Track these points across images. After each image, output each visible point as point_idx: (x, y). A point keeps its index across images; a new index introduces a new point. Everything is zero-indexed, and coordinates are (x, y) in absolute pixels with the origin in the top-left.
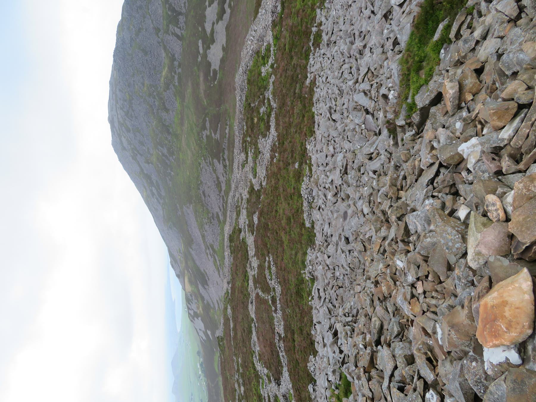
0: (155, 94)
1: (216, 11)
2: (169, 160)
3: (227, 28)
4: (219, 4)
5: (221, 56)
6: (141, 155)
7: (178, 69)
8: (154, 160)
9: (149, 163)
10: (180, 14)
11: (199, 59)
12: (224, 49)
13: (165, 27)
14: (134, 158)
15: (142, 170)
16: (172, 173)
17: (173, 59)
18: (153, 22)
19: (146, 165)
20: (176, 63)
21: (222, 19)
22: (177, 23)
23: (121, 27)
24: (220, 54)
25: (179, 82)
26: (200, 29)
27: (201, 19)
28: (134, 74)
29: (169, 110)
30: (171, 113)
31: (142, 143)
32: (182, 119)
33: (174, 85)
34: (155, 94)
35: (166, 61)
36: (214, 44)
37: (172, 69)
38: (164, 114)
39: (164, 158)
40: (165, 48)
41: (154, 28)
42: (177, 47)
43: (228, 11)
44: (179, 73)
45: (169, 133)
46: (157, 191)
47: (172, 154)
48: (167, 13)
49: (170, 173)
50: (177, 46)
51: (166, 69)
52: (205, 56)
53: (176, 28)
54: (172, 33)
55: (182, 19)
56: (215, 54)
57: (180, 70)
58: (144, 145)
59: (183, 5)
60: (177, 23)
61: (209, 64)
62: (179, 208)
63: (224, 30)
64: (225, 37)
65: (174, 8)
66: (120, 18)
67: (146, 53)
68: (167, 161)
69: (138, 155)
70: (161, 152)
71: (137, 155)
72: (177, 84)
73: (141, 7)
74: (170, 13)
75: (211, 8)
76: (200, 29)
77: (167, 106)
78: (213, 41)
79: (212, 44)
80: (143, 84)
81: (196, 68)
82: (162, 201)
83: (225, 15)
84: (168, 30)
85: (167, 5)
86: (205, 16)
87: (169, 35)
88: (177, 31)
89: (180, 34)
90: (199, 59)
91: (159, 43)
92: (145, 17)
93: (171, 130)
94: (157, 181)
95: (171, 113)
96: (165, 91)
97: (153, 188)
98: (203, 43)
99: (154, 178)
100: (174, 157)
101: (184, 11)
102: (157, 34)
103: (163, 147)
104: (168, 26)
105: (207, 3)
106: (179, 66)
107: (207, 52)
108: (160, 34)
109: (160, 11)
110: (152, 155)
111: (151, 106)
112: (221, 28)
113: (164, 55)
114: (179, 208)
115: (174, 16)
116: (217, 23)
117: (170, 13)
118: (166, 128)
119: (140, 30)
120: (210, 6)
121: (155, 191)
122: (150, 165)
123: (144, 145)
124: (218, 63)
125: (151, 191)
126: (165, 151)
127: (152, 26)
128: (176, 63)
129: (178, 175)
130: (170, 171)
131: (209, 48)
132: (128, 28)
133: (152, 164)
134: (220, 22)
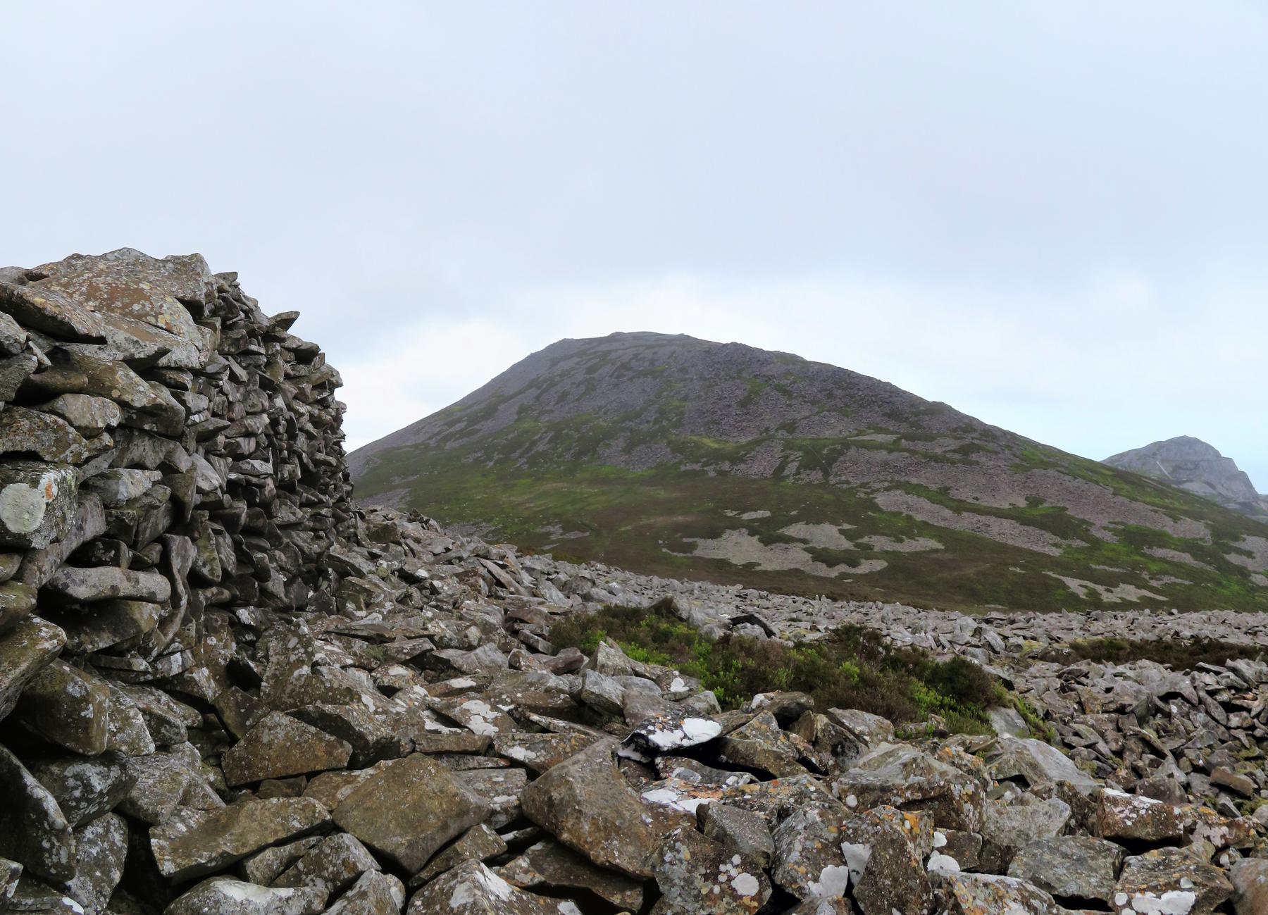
0: (665, 423)
1: (832, 546)
2: (521, 456)
3: (796, 573)
4: (847, 551)
5: (734, 561)
6: (538, 398)
7: (715, 470)
8: (527, 424)
9: (519, 413)
10: (826, 473)
11: (730, 513)
12: (749, 567)
13: (798, 442)
14: (533, 384)
15: (505, 400)
16: (491, 464)
17: (735, 458)
19: (516, 408)
20: (726, 466)
21: (814, 559)
22: (807, 465)
23: (792, 360)
24: (738, 560)
25: (686, 474)
26: (794, 513)
27: (813, 516)
30: (623, 458)
31: (563, 398)
32: (604, 481)
33: (680, 463)
34: (665, 423)
35: (730, 446)
36: (761, 545)
37: (715, 456)
38: (619, 443)
40: (756, 443)
41: (794, 421)
42: (760, 466)
43: (833, 573)
44: (706, 472)
45: (577, 456)
46: (457, 432)
47: (533, 462)
48: (825, 446)
50: (762, 468)
51: (716, 446)
52: (735, 525)
53: (797, 464)
54: (787, 457)
55: (816, 476)
56: (739, 548)
57: (712, 474)
59: (843, 478)
60: (807, 465)
61: (714, 534)
62: (411, 479)
63: (793, 566)
64: (778, 568)
65: (835, 461)
66: (808, 358)
67: (744, 404)
68: (518, 453)
70: (541, 439)
71: (539, 388)
72: (683, 468)
73: (831, 396)
74: (825, 452)
75: (837, 534)
76: (794, 513)
78: (767, 541)
79: (761, 540)
81: (711, 505)
82: (433, 442)
83: (824, 566)
85: (838, 447)
86: (819, 522)
88: (792, 468)
89: (786, 472)
90: (730, 513)
91: (767, 430)
92: (813, 403)
94: (478, 431)
95: (623, 458)
96: (669, 444)
97: (463, 425)
98: (763, 521)
99: (488, 426)
100: (525, 467)
101: (833, 480)
102: (782, 427)
103: (550, 442)
104: (800, 448)
105: (847, 526)
106: (721, 473)
107: (744, 530)
108: (784, 432)
110: (536, 420)
111: (638, 415)
112: (796, 558)
113: (743, 441)
114: (411, 479)
115: (821, 459)
116: (805, 550)
117: (825, 452)
118: (590, 446)
120: (842, 532)
121: (458, 427)
122: (516, 417)
124: (719, 555)
125: (459, 420)
126: (541, 447)
127: (798, 416)
128: (726, 466)
129: (484, 475)
130: (496, 457)
131: (752, 534)
132: (789, 373)
133: (517, 420)
134: (808, 556)
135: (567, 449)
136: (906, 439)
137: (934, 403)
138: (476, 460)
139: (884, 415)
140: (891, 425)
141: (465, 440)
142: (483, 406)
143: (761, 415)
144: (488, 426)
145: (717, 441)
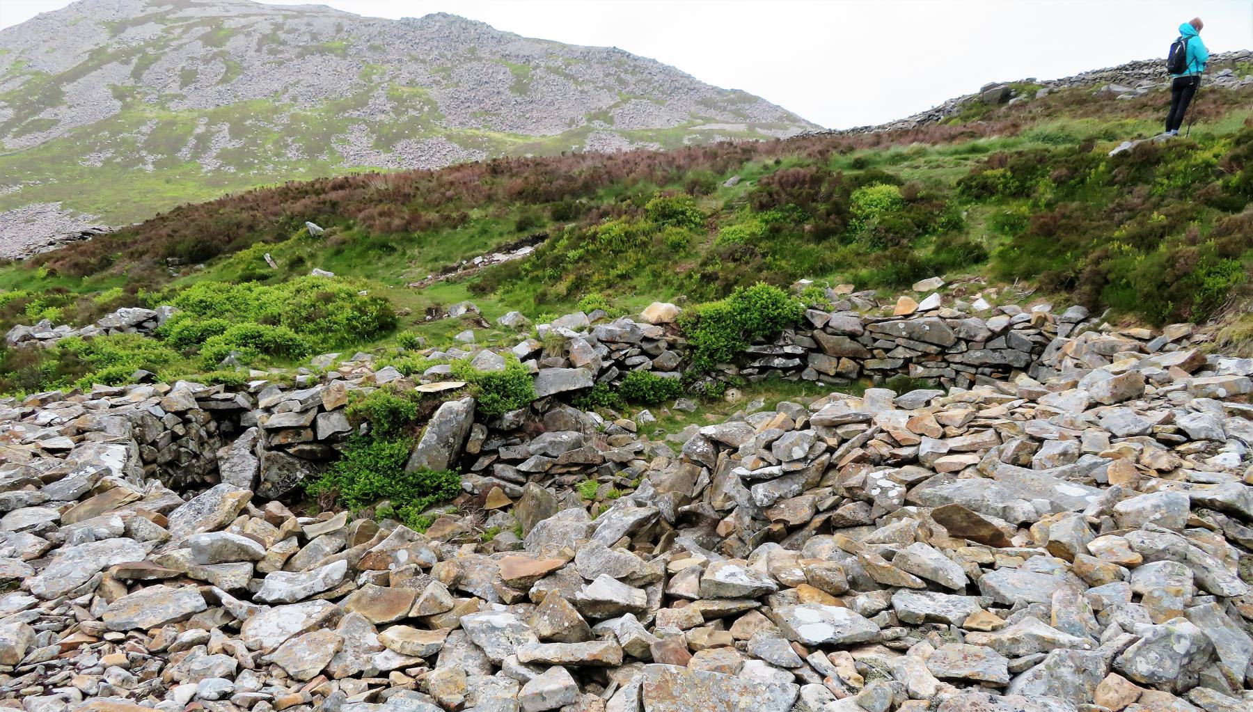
0: (412, 113)
2: (196, 156)
6: (136, 74)
8: (153, 114)
14: (98, 58)
18: (616, 105)
19: (104, 91)
28: (423, 61)
29: (389, 150)
31: (188, 78)
34: (412, 113)
39: (192, 142)
45: (312, 151)
49: (142, 160)
51: (520, 141)
58: (184, 84)
67: (521, 87)
68: (185, 153)
69: (131, 67)
71: (127, 63)
73: (621, 82)
77: (399, 146)
80: (411, 83)
84: (642, 140)
87: (631, 143)
91: (572, 120)
92: (610, 89)
93: (324, 158)
94: (54, 123)
103: (236, 133)
109: (657, 124)
111: (360, 103)
119: (576, 80)
123: (184, 84)
126: (224, 140)
133: (126, 107)
135: (281, 145)
136: (762, 126)
137: (734, 91)
138: (107, 162)
139: (697, 103)
140: (712, 113)
141: (40, 137)
142: (16, 85)
143: (552, 103)
144: (68, 117)
145: (516, 136)
